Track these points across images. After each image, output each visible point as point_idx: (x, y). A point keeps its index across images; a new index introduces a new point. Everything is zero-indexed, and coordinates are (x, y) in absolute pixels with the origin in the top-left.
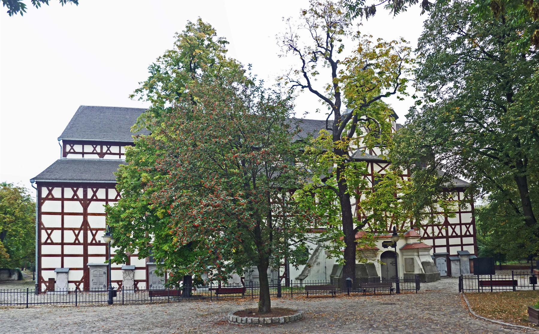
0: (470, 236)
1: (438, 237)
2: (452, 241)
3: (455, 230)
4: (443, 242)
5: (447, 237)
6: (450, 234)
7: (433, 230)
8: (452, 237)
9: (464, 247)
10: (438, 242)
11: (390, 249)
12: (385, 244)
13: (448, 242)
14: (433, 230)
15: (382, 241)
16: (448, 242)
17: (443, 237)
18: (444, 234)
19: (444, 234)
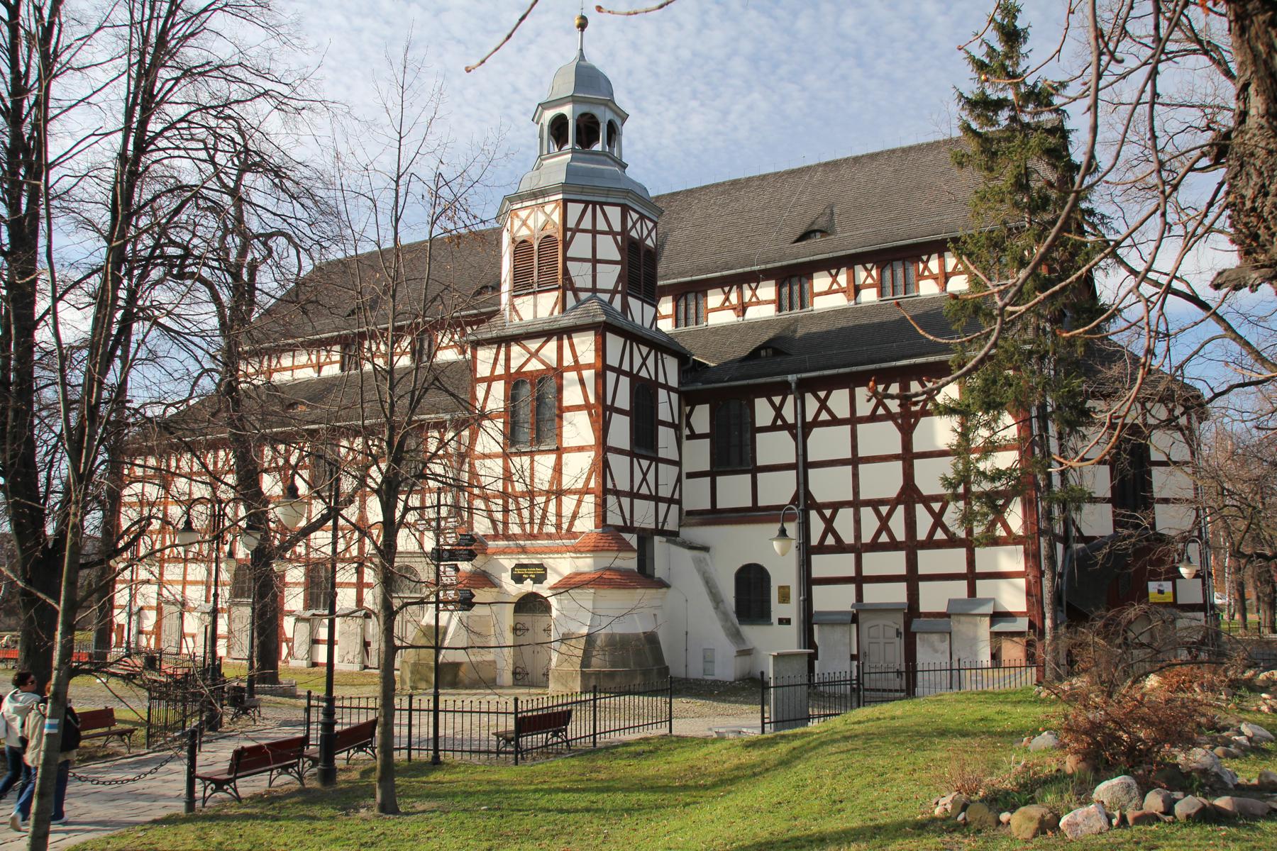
0: (1012, 539)
1: (875, 546)
2: (929, 561)
3: (836, 525)
4: (895, 562)
5: (912, 546)
6: (922, 535)
7: (857, 521)
8: (930, 544)
9: (979, 583)
10: (875, 563)
11: (528, 586)
12: (518, 571)
13: (912, 563)
14: (857, 521)
15: (514, 562)
16: (912, 563)
17: (893, 545)
18: (900, 535)
19: (900, 535)
